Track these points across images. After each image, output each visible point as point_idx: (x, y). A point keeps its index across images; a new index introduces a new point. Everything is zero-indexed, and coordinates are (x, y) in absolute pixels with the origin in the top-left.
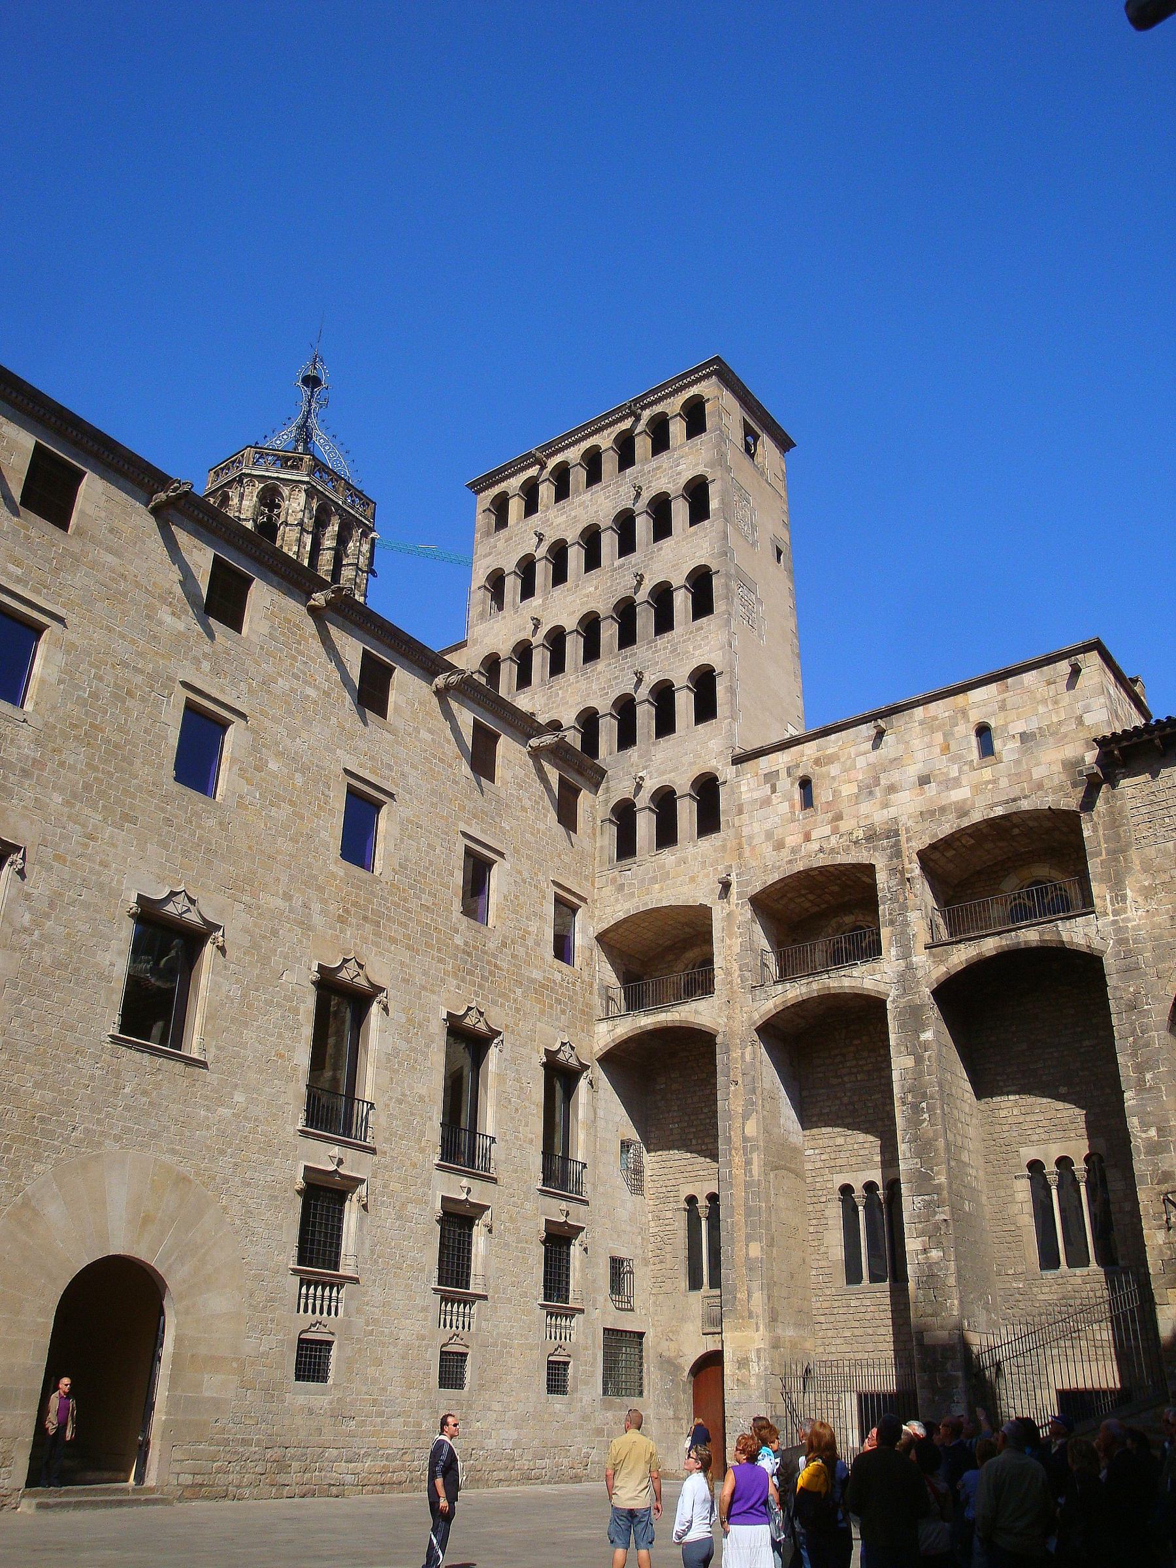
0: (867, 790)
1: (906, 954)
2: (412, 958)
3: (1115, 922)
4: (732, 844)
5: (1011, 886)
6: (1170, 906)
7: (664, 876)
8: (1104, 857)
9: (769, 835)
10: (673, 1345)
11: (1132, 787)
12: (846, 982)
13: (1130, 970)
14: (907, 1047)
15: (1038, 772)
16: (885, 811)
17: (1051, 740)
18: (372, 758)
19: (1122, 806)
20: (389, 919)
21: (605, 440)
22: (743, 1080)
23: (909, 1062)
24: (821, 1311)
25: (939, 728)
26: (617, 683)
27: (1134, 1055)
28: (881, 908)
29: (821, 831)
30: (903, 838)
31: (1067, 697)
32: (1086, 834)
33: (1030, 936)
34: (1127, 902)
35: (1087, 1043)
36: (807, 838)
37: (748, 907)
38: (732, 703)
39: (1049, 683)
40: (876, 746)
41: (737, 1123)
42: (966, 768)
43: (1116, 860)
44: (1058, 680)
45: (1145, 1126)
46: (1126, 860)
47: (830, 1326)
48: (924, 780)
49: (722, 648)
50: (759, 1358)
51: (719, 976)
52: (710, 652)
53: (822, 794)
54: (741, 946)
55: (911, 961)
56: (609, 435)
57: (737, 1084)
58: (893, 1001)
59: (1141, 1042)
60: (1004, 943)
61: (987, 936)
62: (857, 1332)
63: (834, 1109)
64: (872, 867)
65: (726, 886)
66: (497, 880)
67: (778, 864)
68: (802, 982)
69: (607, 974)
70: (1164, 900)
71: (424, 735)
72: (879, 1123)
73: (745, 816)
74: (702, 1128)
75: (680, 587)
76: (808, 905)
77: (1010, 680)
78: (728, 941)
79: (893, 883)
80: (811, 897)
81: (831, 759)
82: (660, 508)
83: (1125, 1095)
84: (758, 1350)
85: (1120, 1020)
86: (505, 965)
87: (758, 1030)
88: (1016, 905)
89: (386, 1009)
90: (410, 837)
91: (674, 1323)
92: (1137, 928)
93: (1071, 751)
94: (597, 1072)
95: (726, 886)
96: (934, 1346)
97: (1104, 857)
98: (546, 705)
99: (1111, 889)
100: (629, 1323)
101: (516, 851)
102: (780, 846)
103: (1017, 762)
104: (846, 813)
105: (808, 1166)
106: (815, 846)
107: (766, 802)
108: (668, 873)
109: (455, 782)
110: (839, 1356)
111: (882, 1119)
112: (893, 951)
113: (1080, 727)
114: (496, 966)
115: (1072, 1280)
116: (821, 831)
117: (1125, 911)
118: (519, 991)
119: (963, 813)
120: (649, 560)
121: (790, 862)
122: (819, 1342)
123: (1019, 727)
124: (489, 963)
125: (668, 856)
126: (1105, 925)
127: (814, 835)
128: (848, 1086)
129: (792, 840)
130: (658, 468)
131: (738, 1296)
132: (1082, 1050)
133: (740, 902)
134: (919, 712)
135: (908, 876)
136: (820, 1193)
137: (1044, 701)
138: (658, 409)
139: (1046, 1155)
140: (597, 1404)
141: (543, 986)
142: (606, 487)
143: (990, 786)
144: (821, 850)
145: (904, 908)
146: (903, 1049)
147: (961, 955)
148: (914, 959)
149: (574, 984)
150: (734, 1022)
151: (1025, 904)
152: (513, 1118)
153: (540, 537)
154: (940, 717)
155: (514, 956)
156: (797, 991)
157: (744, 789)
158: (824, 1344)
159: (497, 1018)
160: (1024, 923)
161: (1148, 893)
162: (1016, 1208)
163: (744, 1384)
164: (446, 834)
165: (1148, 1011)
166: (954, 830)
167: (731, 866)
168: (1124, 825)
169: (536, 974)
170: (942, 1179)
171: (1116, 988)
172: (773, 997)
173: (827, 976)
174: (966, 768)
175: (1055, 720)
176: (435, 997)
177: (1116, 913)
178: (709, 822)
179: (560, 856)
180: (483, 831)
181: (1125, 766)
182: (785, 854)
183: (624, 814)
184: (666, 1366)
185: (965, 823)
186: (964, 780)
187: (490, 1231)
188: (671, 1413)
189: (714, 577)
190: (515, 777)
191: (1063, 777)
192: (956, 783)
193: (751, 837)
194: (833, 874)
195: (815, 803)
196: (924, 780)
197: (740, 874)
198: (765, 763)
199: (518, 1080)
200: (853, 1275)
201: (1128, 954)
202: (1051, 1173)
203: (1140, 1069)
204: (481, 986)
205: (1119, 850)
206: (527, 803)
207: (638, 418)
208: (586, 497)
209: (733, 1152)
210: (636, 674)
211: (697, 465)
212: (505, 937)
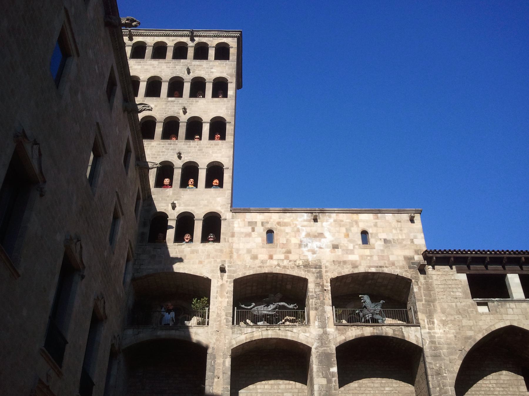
1: (323, 326)
3: (429, 333)
6: (454, 331)
8: (424, 302)
13: (436, 356)
14: (323, 374)
15: (392, 258)
21: (171, 42)
22: (223, 377)
23: (324, 381)
25: (343, 226)
26: (164, 155)
28: (311, 300)
29: (279, 256)
30: (324, 270)
32: (415, 289)
35: (387, 389)
36: (271, 257)
37: (233, 284)
39: (398, 221)
42: (357, 247)
43: (429, 305)
44: (402, 221)
46: (434, 306)
48: (335, 247)
54: (228, 303)
55: (326, 330)
56: (173, 41)
57: (219, 378)
58: (316, 349)
59: (443, 391)
60: (375, 331)
61: (367, 326)
67: (253, 266)
68: (263, 329)
70: (452, 328)
73: (235, 239)
77: (379, 215)
78: (220, 299)
79: (318, 290)
81: (286, 224)
85: (433, 379)
88: (350, 317)
92: (440, 338)
93: (409, 253)
99: (427, 318)
102: (255, 257)
103: (382, 251)
106: (275, 263)
107: (248, 235)
112: (317, 323)
113: (412, 244)
116: (279, 256)
117: (434, 328)
119: (355, 266)
120: (190, 104)
121: (260, 267)
123: (383, 236)
126: (425, 333)
127: (275, 257)
128: (259, 391)
129: (263, 256)
130: (200, 66)
132: (385, 392)
133: (229, 280)
134: (334, 215)
135: (326, 288)
137: (396, 229)
142: (168, 63)
143: (369, 258)
144: (278, 265)
145: (323, 304)
146: (320, 374)
150: (220, 343)
151: (355, 318)
154: (345, 221)
157: (236, 225)
161: (444, 323)
165: (446, 377)
166: (350, 273)
167: (225, 261)
168: (432, 291)
171: (430, 363)
172: (245, 334)
173: (278, 328)
174: (357, 247)
175: (400, 237)
177: (429, 329)
182: (258, 262)
185: (356, 271)
186: (356, 251)
192: (352, 252)
196: (335, 247)
197: (230, 266)
201: (436, 349)
205: (430, 302)
208: (155, 62)
211: (223, 72)
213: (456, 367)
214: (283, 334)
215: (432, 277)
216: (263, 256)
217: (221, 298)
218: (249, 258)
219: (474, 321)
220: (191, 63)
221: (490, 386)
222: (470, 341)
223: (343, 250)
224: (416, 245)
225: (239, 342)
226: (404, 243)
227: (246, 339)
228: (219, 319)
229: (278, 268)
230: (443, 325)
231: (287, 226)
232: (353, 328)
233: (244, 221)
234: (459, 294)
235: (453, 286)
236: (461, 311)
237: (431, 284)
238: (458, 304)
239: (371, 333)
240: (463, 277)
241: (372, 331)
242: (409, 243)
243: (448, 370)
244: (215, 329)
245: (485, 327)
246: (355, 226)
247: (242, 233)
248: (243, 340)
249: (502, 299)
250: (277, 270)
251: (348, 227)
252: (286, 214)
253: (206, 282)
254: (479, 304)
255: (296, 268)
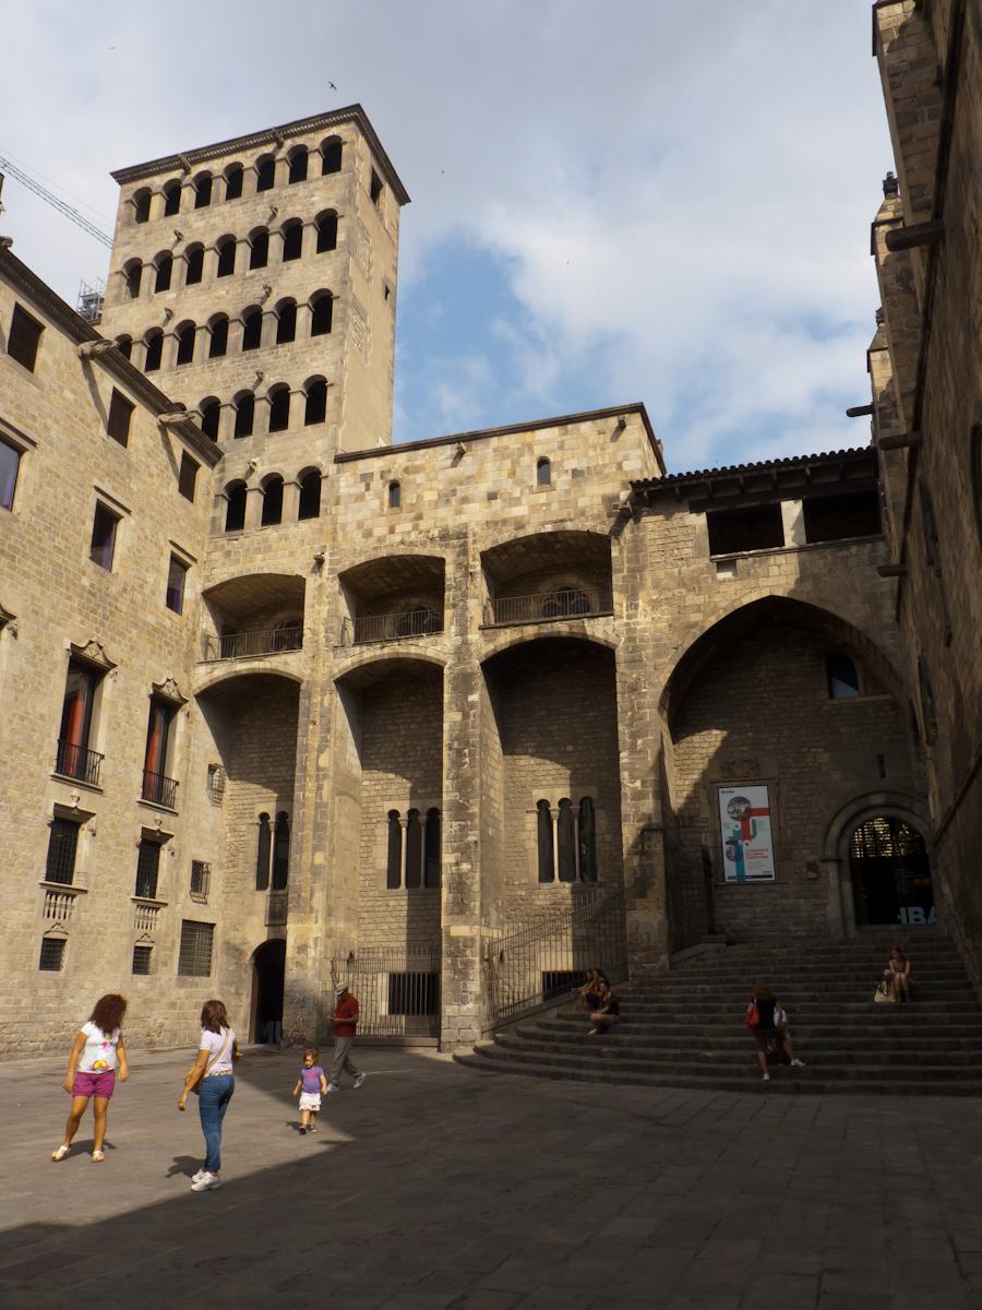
0: (445, 498)
1: (463, 632)
2: (43, 593)
3: (627, 624)
4: (328, 528)
5: (547, 588)
7: (267, 549)
8: (625, 574)
9: (360, 525)
10: (239, 935)
11: (652, 524)
12: (413, 650)
13: (635, 662)
15: (582, 502)
16: (458, 517)
17: (596, 478)
18: (18, 407)
19: (644, 536)
20: (25, 555)
21: (248, 159)
23: (458, 717)
24: (365, 909)
25: (509, 457)
27: (631, 725)
28: (447, 594)
29: (404, 526)
30: (470, 540)
31: (611, 447)
32: (614, 554)
33: (562, 627)
34: (640, 609)
35: (590, 714)
36: (392, 530)
37: (337, 581)
38: (338, 411)
39: (600, 433)
40: (454, 465)
41: (313, 756)
43: (634, 577)
45: (633, 778)
47: (370, 921)
48: (492, 496)
49: (336, 363)
50: (316, 944)
51: (307, 634)
52: (324, 365)
53: (408, 497)
56: (252, 155)
58: (450, 668)
59: (637, 716)
61: (528, 624)
62: (393, 926)
63: (389, 750)
64: (444, 560)
65: (320, 562)
66: (124, 533)
67: (365, 549)
69: (207, 624)
71: (68, 395)
72: (424, 764)
73: (341, 507)
74: (278, 758)
75: (304, 305)
76: (384, 585)
77: (570, 426)
78: (317, 607)
79: (458, 574)
80: (388, 580)
81: (417, 470)
82: (293, 231)
83: (622, 755)
84: (316, 939)
86: (124, 608)
87: (336, 682)
89: (15, 635)
90: (49, 484)
91: (242, 916)
92: (644, 630)
94: (193, 706)
95: (320, 562)
96: (458, 937)
97: (625, 574)
98: (171, 389)
99: (628, 600)
100: (202, 915)
101: (141, 511)
102: (368, 534)
103: (568, 492)
104: (426, 514)
105: (365, 794)
106: (397, 538)
107: (360, 498)
108: (271, 546)
109: (92, 441)
110: (376, 945)
111: (427, 761)
112: (453, 629)
114: (116, 608)
115: (562, 891)
116: (404, 526)
117: (635, 616)
118: (134, 632)
119: (520, 526)
121: (375, 549)
122: (362, 933)
123: (572, 464)
124: (110, 604)
125: (271, 532)
126: (620, 625)
128: (402, 733)
129: (379, 531)
131: (303, 894)
134: (494, 442)
136: (372, 816)
137: (594, 447)
138: (300, 141)
139: (552, 797)
140: (173, 983)
141: (155, 630)
143: (544, 508)
144: (403, 542)
145: (465, 596)
147: (506, 638)
148: (470, 637)
149: (181, 631)
152: (121, 740)
153: (179, 237)
155: (132, 601)
156: (370, 653)
157: (342, 484)
158: (365, 935)
159: (114, 652)
160: (559, 617)
161: (655, 605)
162: (524, 835)
163: (301, 965)
164: (82, 486)
169: (151, 619)
170: (475, 809)
171: (623, 674)
174: (527, 491)
175: (601, 463)
176: (60, 629)
177: (629, 617)
178: (310, 506)
179: (178, 520)
180: (115, 489)
181: (649, 505)
182: (372, 542)
183: (236, 494)
184: (231, 951)
185: (521, 534)
186: (524, 500)
187: (94, 835)
188: (233, 990)
189: (334, 302)
190: (145, 446)
191: (602, 508)
192: (517, 502)
193: (344, 525)
194: (407, 562)
195: (401, 503)
196: (492, 496)
198: (363, 466)
199: (128, 708)
200: (393, 882)
201: (635, 649)
202: (554, 810)
203: (634, 736)
204: (102, 624)
205: (637, 570)
206: (154, 471)
207: (280, 145)
209: (308, 779)
210: (257, 373)
211: (329, 199)
212: (126, 583)
213: (664, 677)
214: (405, 651)
215: (645, 527)
216: (379, 531)
217: (320, 605)
218: (360, 536)
219: (707, 596)
220: (279, 194)
221: (765, 695)
222: (693, 631)
223: (504, 501)
224: (626, 473)
225: (343, 670)
226: (606, 471)
227: (353, 664)
228: (316, 638)
229: (402, 546)
230: (653, 608)
231: (419, 472)
232: (508, 631)
233: (355, 474)
234: (687, 552)
235: (680, 538)
236: (686, 581)
237: (642, 541)
238: (684, 569)
239: (535, 635)
240: (699, 521)
241: (536, 632)
242: (615, 470)
243: (650, 683)
244: (311, 655)
245: (723, 604)
246: (527, 454)
247: (351, 495)
248: (347, 668)
249: (761, 551)
250: (401, 551)
251: (516, 457)
252: (418, 452)
253: (299, 582)
254: (721, 566)
255: (428, 543)
